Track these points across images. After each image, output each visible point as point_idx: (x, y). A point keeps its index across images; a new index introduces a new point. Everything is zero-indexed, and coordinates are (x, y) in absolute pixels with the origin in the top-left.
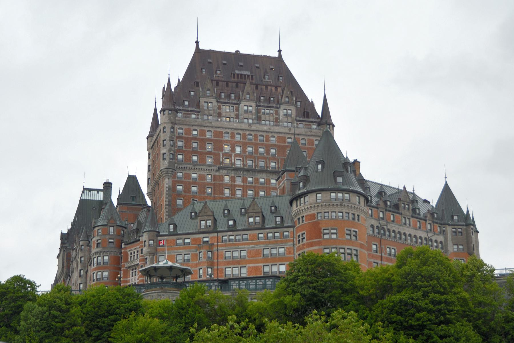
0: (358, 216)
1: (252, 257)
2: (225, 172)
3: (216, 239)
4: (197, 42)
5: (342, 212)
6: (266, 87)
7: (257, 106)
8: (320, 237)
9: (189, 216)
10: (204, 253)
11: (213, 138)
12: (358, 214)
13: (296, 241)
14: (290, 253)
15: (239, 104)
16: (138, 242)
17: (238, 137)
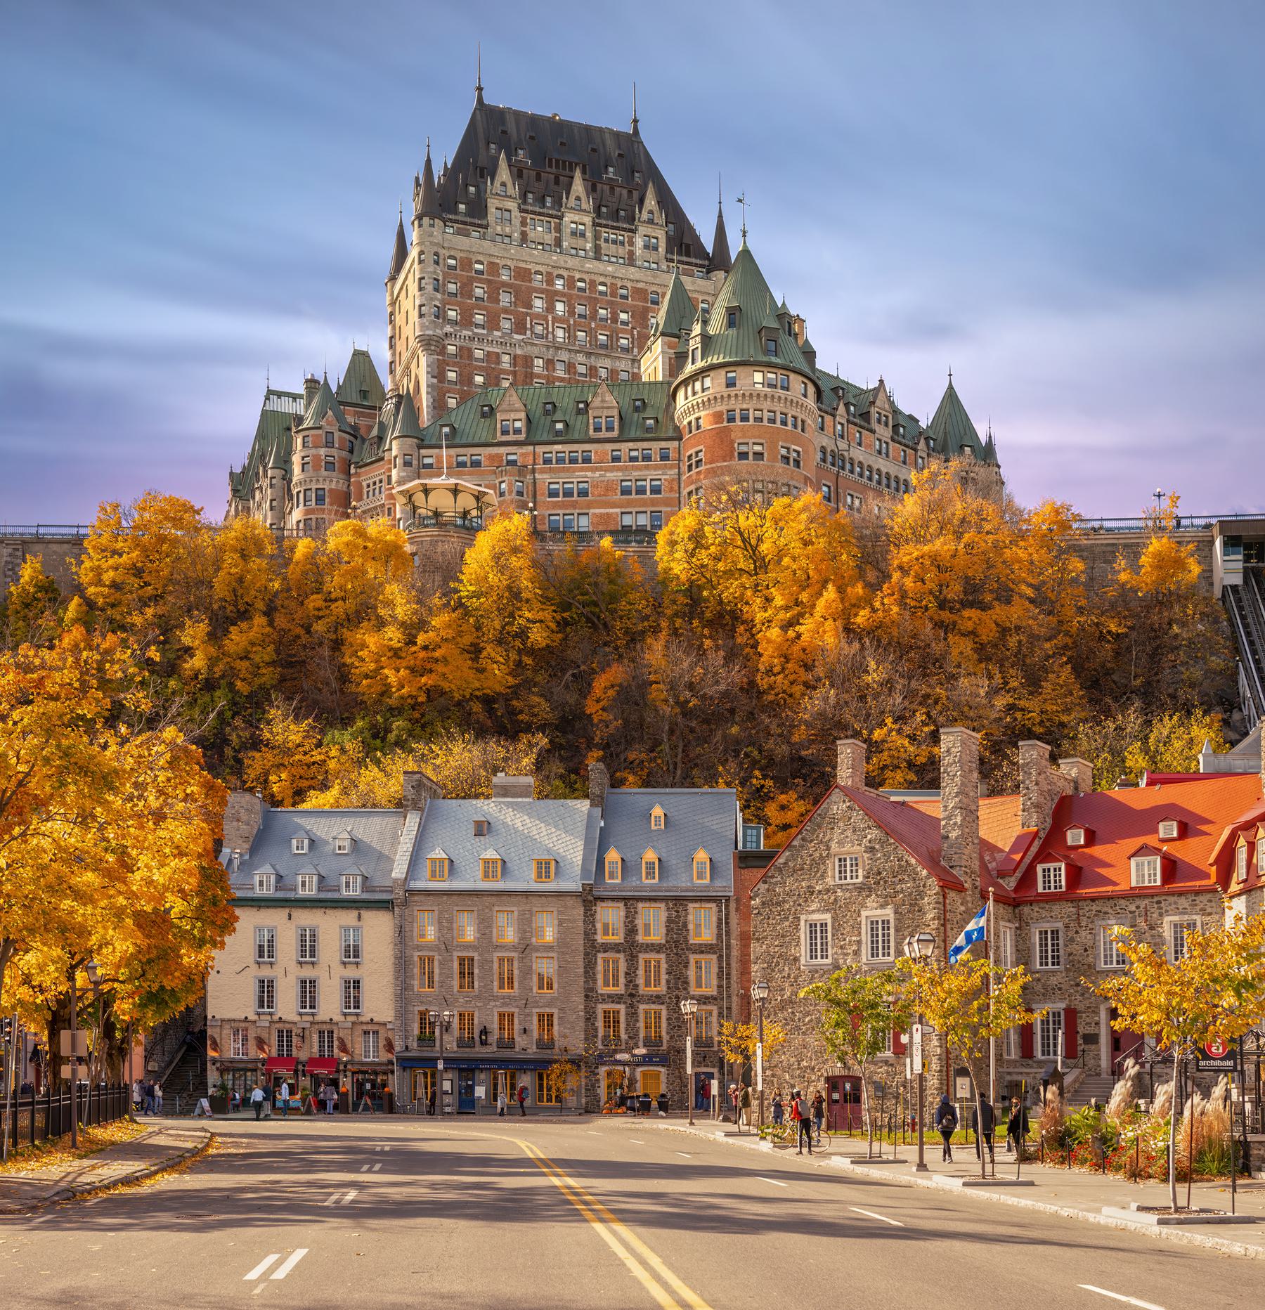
0: (803, 422)
1: (600, 496)
2: (536, 351)
3: (531, 457)
4: (480, 89)
5: (774, 412)
6: (612, 189)
7: (595, 224)
8: (732, 458)
9: (479, 414)
10: (510, 485)
11: (512, 281)
12: (803, 417)
13: (684, 468)
14: (671, 490)
15: (560, 218)
16: (381, 463)
17: (559, 285)
